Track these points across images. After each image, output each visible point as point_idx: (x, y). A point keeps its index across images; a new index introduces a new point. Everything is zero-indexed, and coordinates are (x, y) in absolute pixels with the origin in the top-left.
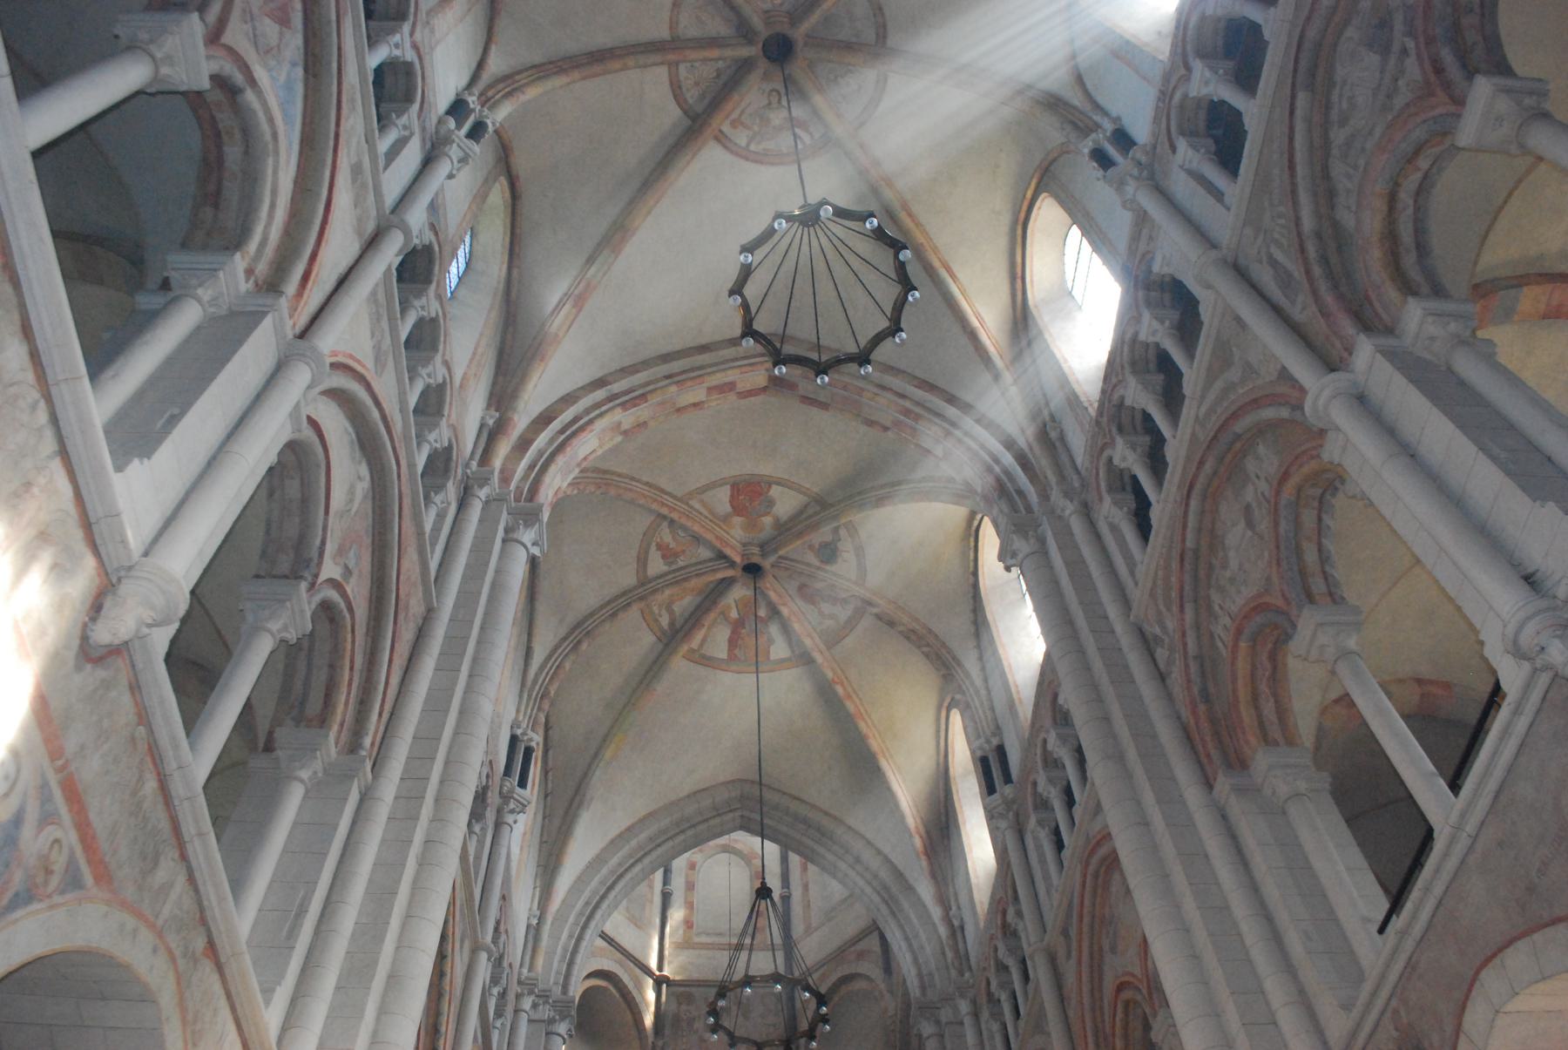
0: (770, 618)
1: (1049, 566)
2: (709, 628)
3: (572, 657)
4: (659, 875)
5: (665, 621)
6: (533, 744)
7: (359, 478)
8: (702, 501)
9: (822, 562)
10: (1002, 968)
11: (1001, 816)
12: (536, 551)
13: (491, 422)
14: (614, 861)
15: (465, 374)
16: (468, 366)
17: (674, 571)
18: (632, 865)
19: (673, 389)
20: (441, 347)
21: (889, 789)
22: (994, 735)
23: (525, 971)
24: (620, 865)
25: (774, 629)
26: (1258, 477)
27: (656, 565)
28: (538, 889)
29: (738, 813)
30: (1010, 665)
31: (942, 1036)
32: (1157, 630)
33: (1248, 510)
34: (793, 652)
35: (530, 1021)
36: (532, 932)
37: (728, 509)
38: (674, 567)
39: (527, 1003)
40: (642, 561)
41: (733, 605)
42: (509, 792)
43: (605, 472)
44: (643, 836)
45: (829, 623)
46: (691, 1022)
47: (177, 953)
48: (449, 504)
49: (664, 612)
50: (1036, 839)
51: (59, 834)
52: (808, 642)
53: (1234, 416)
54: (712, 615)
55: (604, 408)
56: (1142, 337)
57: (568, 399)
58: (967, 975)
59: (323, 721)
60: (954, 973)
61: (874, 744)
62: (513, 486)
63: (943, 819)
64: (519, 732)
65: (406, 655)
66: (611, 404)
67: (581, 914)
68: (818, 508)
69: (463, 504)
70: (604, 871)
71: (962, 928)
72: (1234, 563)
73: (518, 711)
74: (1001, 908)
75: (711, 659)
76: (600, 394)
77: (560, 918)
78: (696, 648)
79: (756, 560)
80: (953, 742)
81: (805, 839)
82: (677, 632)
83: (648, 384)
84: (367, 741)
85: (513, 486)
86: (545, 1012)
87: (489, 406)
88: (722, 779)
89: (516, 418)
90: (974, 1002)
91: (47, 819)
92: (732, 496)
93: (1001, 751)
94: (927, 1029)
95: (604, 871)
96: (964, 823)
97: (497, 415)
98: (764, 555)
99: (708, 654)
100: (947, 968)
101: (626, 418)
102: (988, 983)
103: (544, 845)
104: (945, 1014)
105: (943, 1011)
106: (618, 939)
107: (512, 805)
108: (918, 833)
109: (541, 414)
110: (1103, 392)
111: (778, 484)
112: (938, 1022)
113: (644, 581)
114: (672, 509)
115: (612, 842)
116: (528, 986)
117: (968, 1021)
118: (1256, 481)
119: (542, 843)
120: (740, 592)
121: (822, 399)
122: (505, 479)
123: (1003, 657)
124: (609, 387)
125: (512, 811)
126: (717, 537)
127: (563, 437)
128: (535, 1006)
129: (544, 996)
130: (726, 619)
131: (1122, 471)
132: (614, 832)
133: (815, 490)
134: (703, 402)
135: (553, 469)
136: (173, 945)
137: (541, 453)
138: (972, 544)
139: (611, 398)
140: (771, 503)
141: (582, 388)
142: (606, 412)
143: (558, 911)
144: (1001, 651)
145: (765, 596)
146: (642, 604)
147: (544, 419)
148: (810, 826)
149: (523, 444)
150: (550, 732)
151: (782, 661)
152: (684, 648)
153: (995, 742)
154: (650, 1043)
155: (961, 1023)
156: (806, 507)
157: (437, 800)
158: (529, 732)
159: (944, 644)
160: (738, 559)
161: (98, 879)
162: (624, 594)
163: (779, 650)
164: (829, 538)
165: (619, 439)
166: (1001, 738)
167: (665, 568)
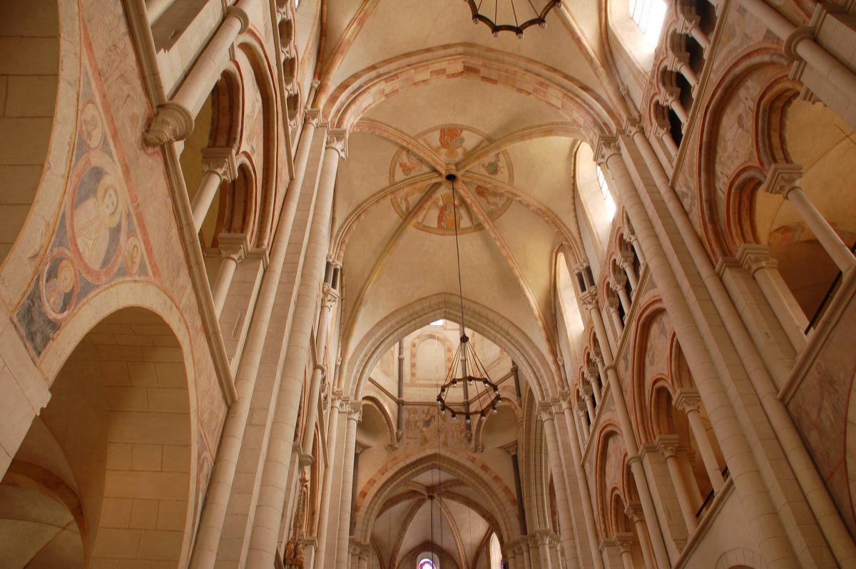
0: (461, 205)
1: (622, 162)
2: (427, 212)
3: (356, 223)
4: (397, 345)
5: (404, 206)
6: (338, 267)
7: (257, 100)
8: (425, 140)
9: (490, 173)
10: (586, 383)
11: (590, 303)
12: (342, 154)
13: (316, 86)
14: (380, 333)
15: (303, 57)
16: (304, 54)
17: (408, 179)
18: (388, 337)
19: (413, 71)
20: (293, 37)
21: (525, 296)
22: (585, 261)
23: (336, 387)
24: (382, 336)
25: (462, 212)
26: (747, 99)
27: (399, 175)
28: (340, 348)
29: (443, 310)
30: (594, 225)
31: (553, 420)
32: (684, 189)
33: (740, 117)
35: (339, 412)
36: (338, 368)
37: (439, 144)
38: (410, 176)
39: (337, 403)
40: (392, 173)
42: (327, 291)
43: (373, 121)
44: (393, 321)
46: (416, 422)
47: (189, 324)
48: (297, 126)
50: (608, 313)
51: (137, 243)
52: (481, 218)
53: (735, 65)
54: (429, 203)
55: (375, 81)
56: (679, 31)
57: (356, 76)
58: (566, 389)
59: (243, 228)
60: (559, 388)
61: (517, 272)
62: (329, 120)
63: (553, 311)
64: (331, 260)
65: (282, 201)
66: (379, 79)
67: (362, 360)
68: (488, 143)
69: (304, 127)
70: (373, 339)
71: (564, 366)
72: (730, 146)
73: (329, 250)
74: (587, 352)
76: (373, 74)
77: (352, 363)
78: (420, 221)
79: (453, 172)
81: (479, 324)
82: (410, 213)
83: (399, 69)
84: (266, 242)
85: (329, 120)
86: (347, 408)
87: (314, 77)
88: (434, 293)
89: (329, 83)
90: (570, 402)
91: (131, 233)
92: (441, 137)
93: (588, 270)
94: (545, 416)
95: (373, 339)
96: (565, 312)
97: (319, 82)
98: (457, 170)
99: (427, 225)
100: (556, 386)
101: (388, 87)
102: (578, 391)
103: (342, 325)
104: (554, 409)
105: (553, 408)
106: (377, 381)
107: (329, 297)
108: (540, 317)
109: (341, 84)
110: (654, 65)
111: (466, 129)
112: (551, 413)
113: (393, 184)
114: (409, 143)
115: (377, 324)
116: (338, 395)
117: (567, 412)
118: (745, 101)
119: (341, 324)
120: (444, 191)
121: (493, 78)
122: (325, 116)
123: (590, 220)
124: (378, 70)
125: (330, 301)
126: (433, 160)
127: (354, 96)
128: (341, 405)
129: (346, 400)
131: (663, 107)
132: (377, 320)
133: (487, 133)
134: (428, 80)
135: (350, 112)
136: (188, 321)
137: (343, 104)
138: (573, 162)
139: (379, 76)
140: (462, 140)
141: (364, 70)
142: (376, 83)
143: (351, 359)
144: (589, 217)
145: (458, 193)
146: (392, 196)
147: (344, 86)
148: (482, 317)
149: (333, 99)
152: (414, 221)
153: (585, 265)
154: (395, 434)
155: (563, 413)
156: (482, 142)
157: (302, 276)
158: (337, 262)
159: (556, 216)
160: (443, 172)
161: (154, 274)
162: (383, 190)
163: (465, 222)
164: (493, 160)
165: (383, 99)
166: (589, 263)
167: (405, 177)
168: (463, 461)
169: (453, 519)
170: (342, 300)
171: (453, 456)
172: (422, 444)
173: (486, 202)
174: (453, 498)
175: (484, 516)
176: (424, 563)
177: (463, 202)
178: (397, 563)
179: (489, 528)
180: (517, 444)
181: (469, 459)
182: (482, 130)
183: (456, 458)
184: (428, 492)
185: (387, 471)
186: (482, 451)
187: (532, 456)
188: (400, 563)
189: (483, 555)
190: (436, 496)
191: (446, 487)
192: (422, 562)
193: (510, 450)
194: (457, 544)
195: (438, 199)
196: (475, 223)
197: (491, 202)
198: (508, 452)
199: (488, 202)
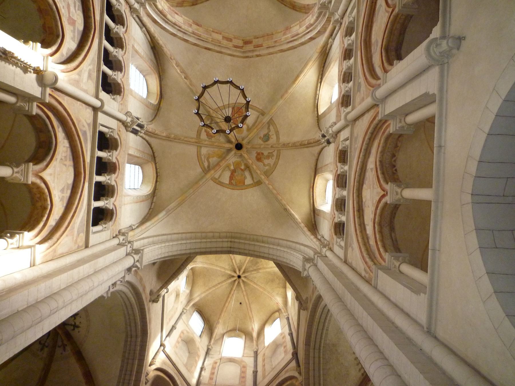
0: (245, 169)
2: (223, 171)
25: (247, 174)
34: (254, 181)
41: (232, 164)
45: (267, 167)
49: (206, 161)
75: (223, 183)
78: (217, 178)
80: (316, 198)
99: (222, 181)
106: (177, 364)
130: (229, 169)
150: (156, 191)
151: (249, 185)
156: (258, 117)
160: (233, 140)
163: (248, 181)
164: (265, 131)
170: (150, 209)
173: (263, 164)
177: (247, 167)
182: (258, 107)
195: (230, 164)
196: (255, 181)
197: (266, 164)
199: (264, 165)
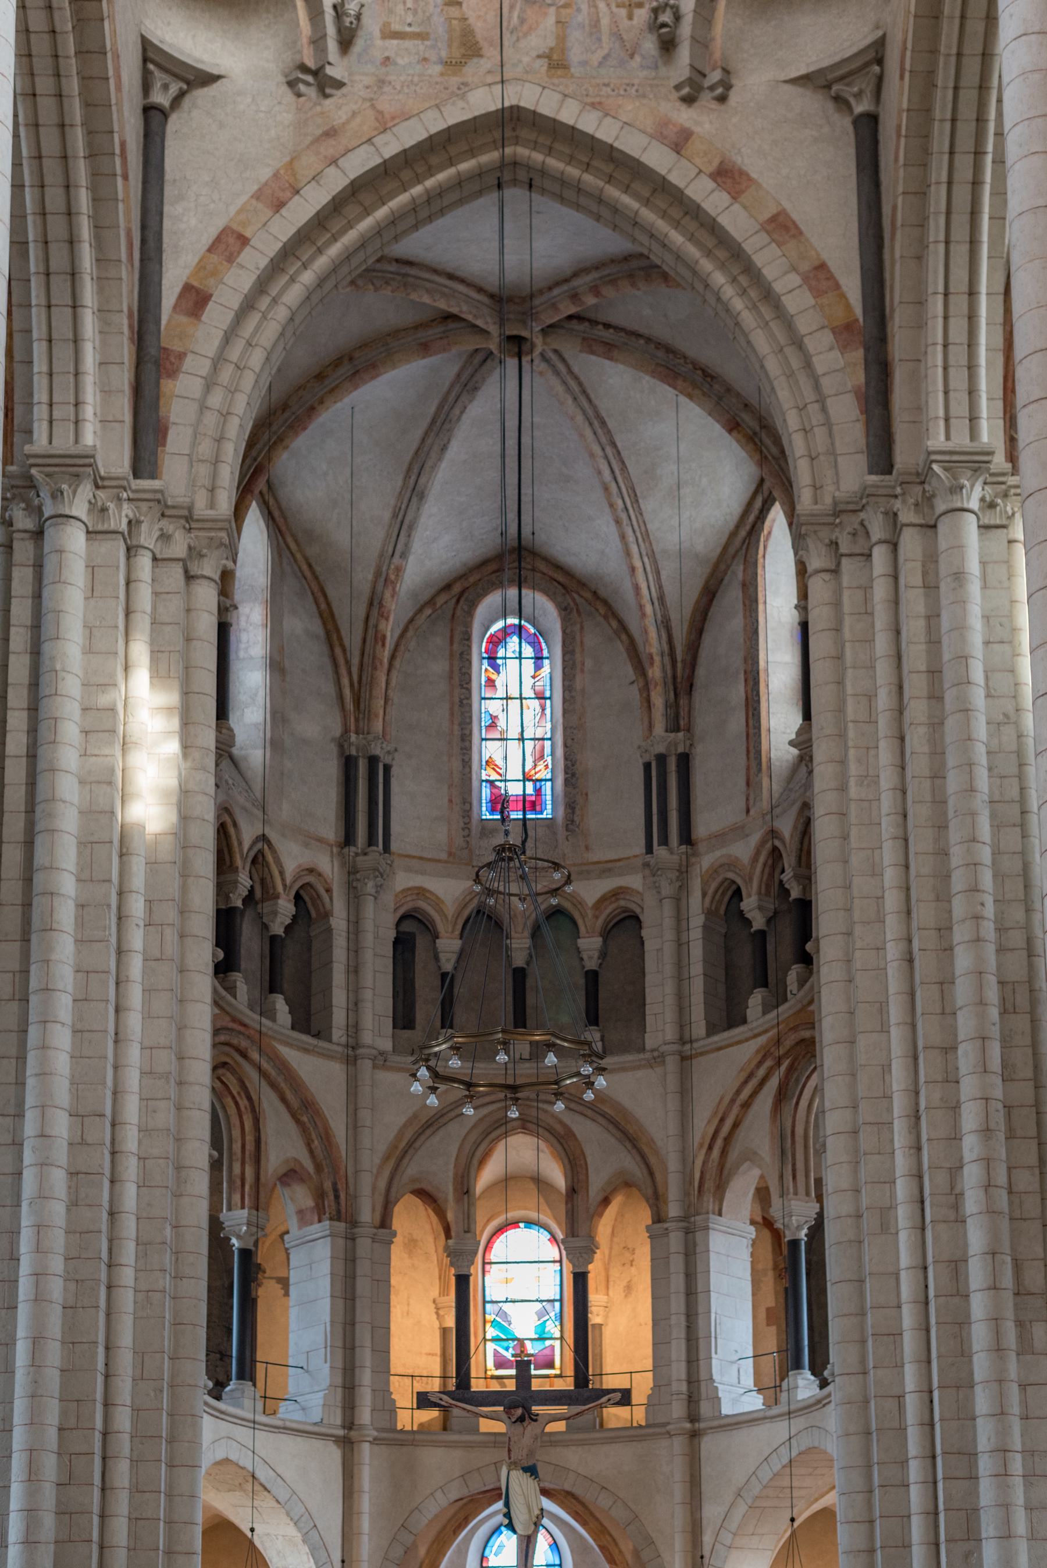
168: (632, 144)
169: (614, 444)
171: (589, 123)
172: (453, 65)
174: (609, 350)
175: (733, 426)
176: (506, 632)
178: (390, 629)
179: (762, 481)
180: (880, 61)
181: (659, 135)
183: (606, 131)
184: (502, 323)
185: (298, 192)
186: (722, 99)
187: (941, 109)
188: (402, 636)
189: (731, 596)
190: (538, 341)
191: (575, 297)
192: (493, 629)
193: (848, 91)
194: (628, 554)
198: (840, 101)
